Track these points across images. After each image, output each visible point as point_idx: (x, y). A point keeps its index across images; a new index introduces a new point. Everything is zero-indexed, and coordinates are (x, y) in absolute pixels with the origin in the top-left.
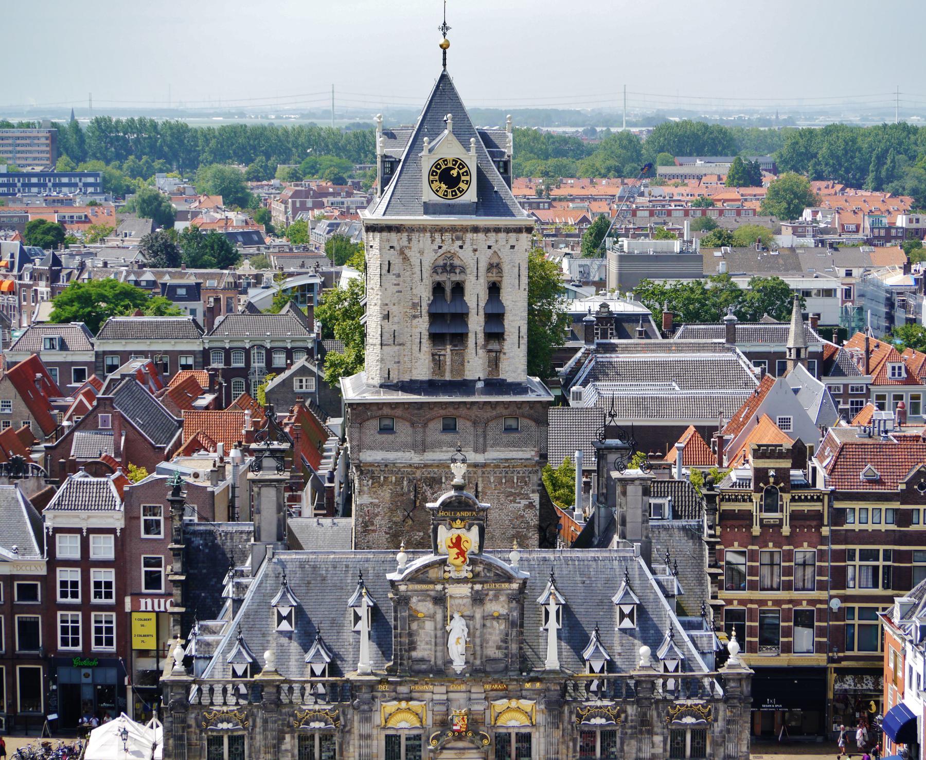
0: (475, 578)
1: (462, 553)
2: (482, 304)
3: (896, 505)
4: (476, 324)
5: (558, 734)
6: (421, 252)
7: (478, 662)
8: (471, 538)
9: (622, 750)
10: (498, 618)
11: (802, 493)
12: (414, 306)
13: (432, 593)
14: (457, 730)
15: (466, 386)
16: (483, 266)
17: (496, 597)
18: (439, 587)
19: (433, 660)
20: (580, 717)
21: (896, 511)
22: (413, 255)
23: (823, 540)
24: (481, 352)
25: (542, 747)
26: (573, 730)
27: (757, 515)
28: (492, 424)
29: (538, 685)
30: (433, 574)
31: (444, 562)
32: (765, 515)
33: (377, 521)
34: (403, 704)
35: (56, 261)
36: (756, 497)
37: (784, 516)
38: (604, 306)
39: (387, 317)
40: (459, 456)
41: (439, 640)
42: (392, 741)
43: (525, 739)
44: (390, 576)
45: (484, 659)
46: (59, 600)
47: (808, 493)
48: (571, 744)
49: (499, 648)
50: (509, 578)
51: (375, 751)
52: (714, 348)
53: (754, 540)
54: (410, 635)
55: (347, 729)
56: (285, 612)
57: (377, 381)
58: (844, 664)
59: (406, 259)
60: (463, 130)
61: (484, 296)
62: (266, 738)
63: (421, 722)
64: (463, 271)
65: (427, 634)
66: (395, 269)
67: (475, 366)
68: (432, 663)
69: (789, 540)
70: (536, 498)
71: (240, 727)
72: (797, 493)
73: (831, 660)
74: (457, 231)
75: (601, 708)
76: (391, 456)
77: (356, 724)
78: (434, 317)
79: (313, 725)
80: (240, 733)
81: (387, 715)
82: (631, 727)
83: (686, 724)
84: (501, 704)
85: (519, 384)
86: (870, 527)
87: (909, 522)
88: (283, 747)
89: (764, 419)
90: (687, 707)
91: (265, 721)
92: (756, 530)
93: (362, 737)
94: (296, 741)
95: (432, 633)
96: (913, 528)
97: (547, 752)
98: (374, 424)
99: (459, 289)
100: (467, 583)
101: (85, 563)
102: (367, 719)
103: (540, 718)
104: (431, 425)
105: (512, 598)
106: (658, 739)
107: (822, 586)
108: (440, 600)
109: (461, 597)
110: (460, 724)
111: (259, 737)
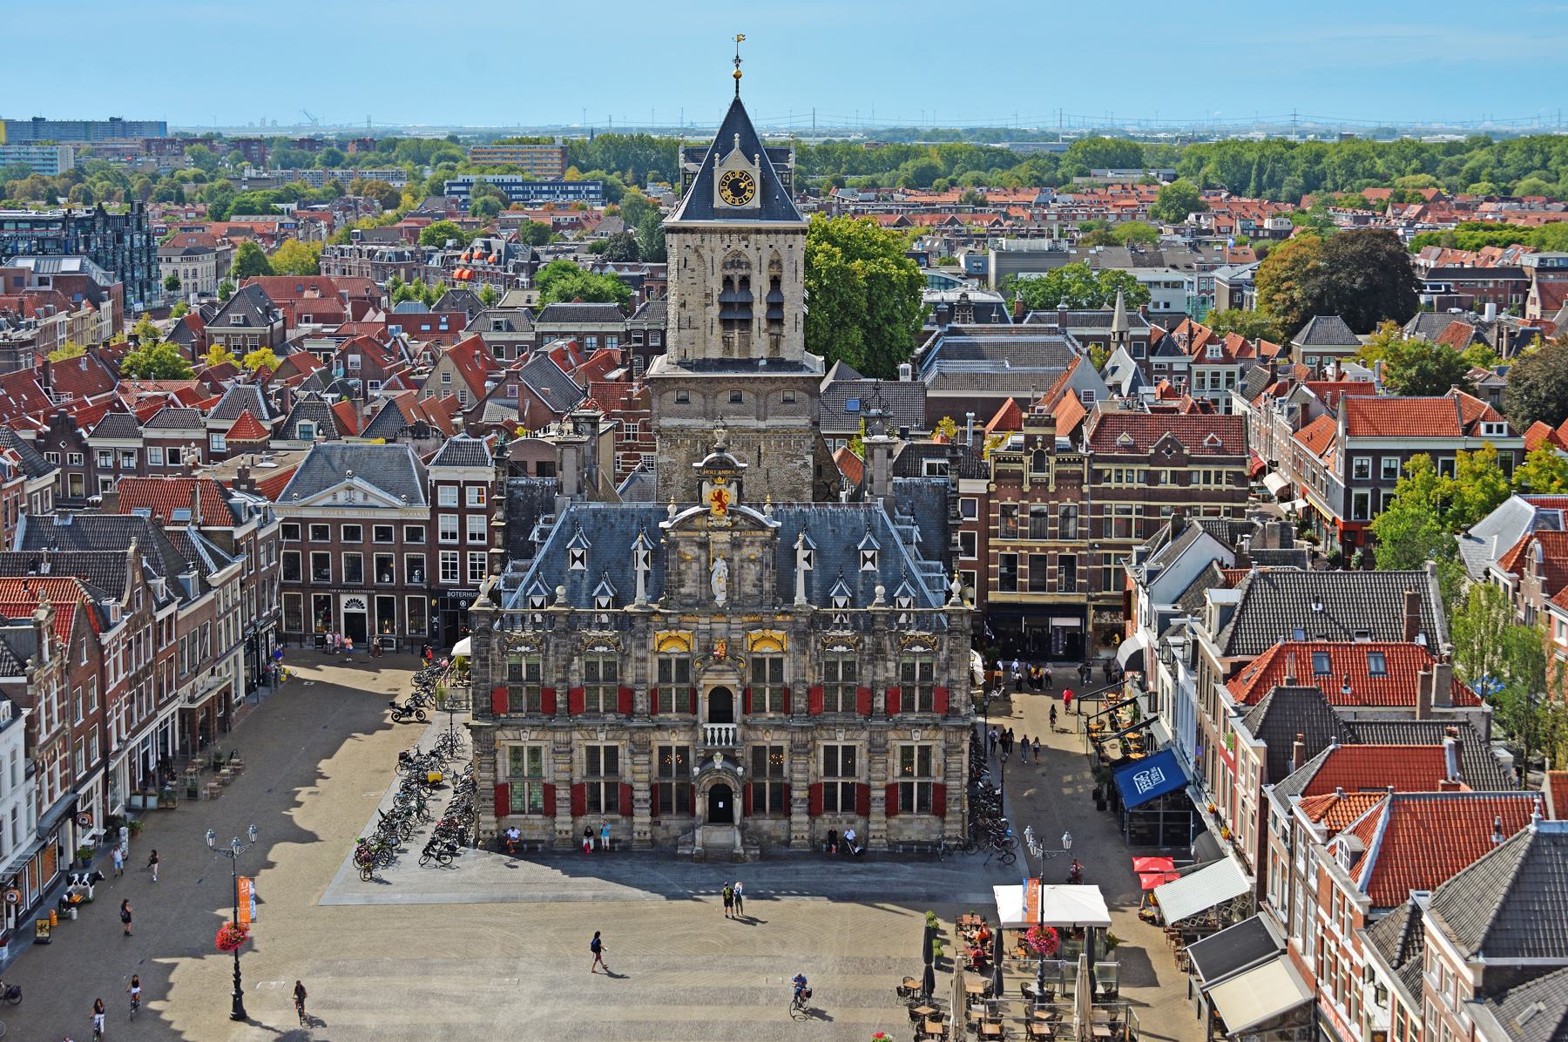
0: (734, 526)
1: (722, 505)
2: (765, 295)
3: (1146, 467)
4: (760, 311)
6: (712, 251)
8: (731, 494)
10: (753, 561)
11: (1066, 456)
12: (707, 295)
15: (750, 364)
16: (765, 263)
17: (752, 543)
18: (703, 534)
20: (824, 645)
21: (1147, 472)
22: (706, 252)
23: (1083, 496)
24: (764, 335)
27: (1028, 475)
28: (772, 396)
30: (697, 522)
31: (707, 513)
32: (1033, 474)
33: (675, 477)
34: (674, 633)
35: (535, 256)
36: (1026, 459)
37: (1051, 475)
38: (964, 295)
39: (683, 305)
40: (720, 423)
42: (664, 665)
43: (777, 664)
44: (663, 525)
46: (441, 541)
47: (1072, 456)
50: (762, 527)
52: (1050, 331)
53: (1024, 495)
54: (679, 574)
56: (578, 553)
57: (675, 360)
58: (1101, 602)
59: (700, 256)
60: (751, 144)
61: (767, 288)
64: (748, 265)
66: (691, 264)
67: (760, 348)
69: (1054, 496)
70: (810, 458)
72: (1061, 456)
73: (1090, 599)
74: (744, 233)
76: (687, 422)
78: (725, 306)
85: (796, 363)
86: (1125, 485)
87: (1157, 482)
89: (1070, 393)
91: (557, 646)
92: (1027, 488)
93: (637, 659)
96: (1160, 487)
98: (672, 396)
99: (745, 281)
101: (462, 511)
102: (644, 646)
103: (788, 645)
104: (720, 397)
105: (764, 544)
106: (891, 665)
107: (1082, 535)
108: (704, 545)
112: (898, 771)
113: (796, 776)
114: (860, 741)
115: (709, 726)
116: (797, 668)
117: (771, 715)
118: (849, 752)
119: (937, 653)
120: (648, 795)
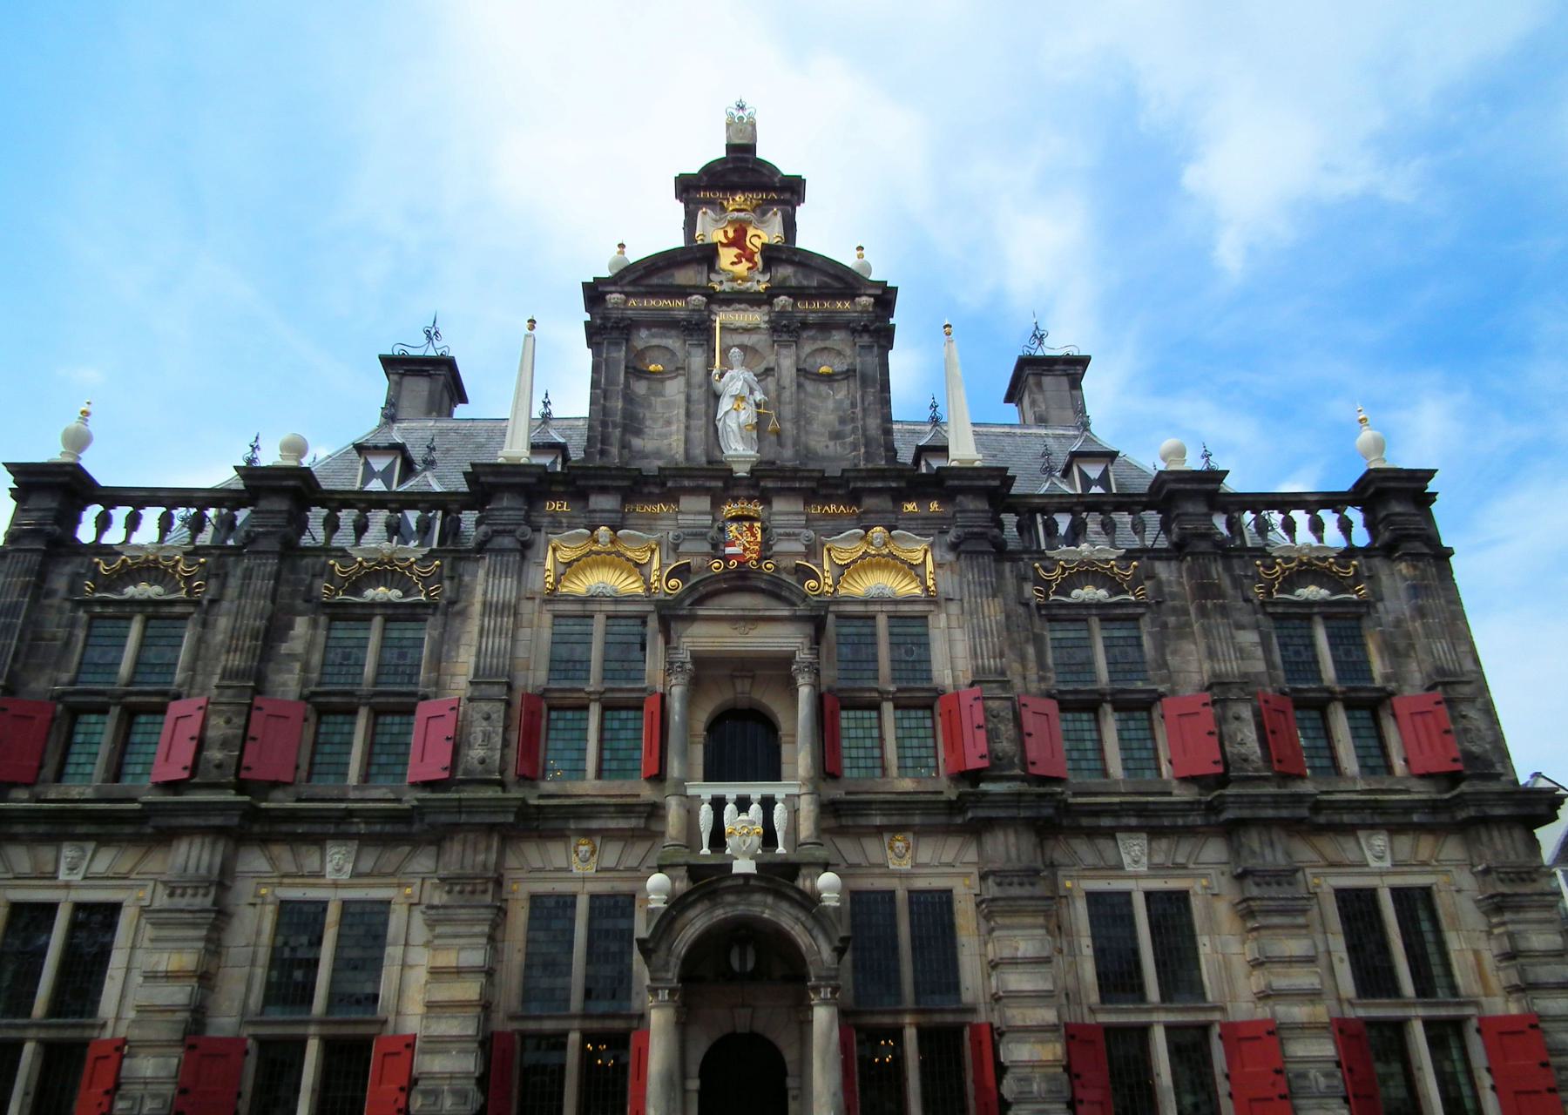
5: (993, 611)
7: (788, 453)
9: (1164, 664)
10: (829, 378)
13: (682, 315)
14: (733, 556)
18: (697, 299)
19: (681, 450)
25: (962, 648)
26: (1031, 616)
29: (934, 506)
30: (684, 277)
41: (699, 408)
45: (803, 452)
48: (1031, 651)
49: (836, 436)
51: (521, 652)
54: (629, 398)
55: (457, 607)
62: (239, 613)
63: (646, 581)
65: (669, 405)
68: (680, 456)
71: (183, 594)
75: (1091, 563)
77: (479, 590)
79: (370, 594)
80: (178, 609)
81: (561, 569)
82: (1174, 611)
83: (1308, 603)
84: (845, 549)
88: (284, 648)
90: (1301, 563)
91: (248, 575)
94: (322, 633)
95: (681, 398)
97: (974, 655)
100: (759, 306)
106: (1249, 638)
109: (746, 330)
110: (743, 540)
111: (223, 623)
112: (1347, 985)
113: (1018, 981)
114: (1205, 876)
115: (707, 791)
116: (979, 633)
117: (907, 784)
118: (1171, 913)
119: (1367, 605)
120: (467, 1063)
